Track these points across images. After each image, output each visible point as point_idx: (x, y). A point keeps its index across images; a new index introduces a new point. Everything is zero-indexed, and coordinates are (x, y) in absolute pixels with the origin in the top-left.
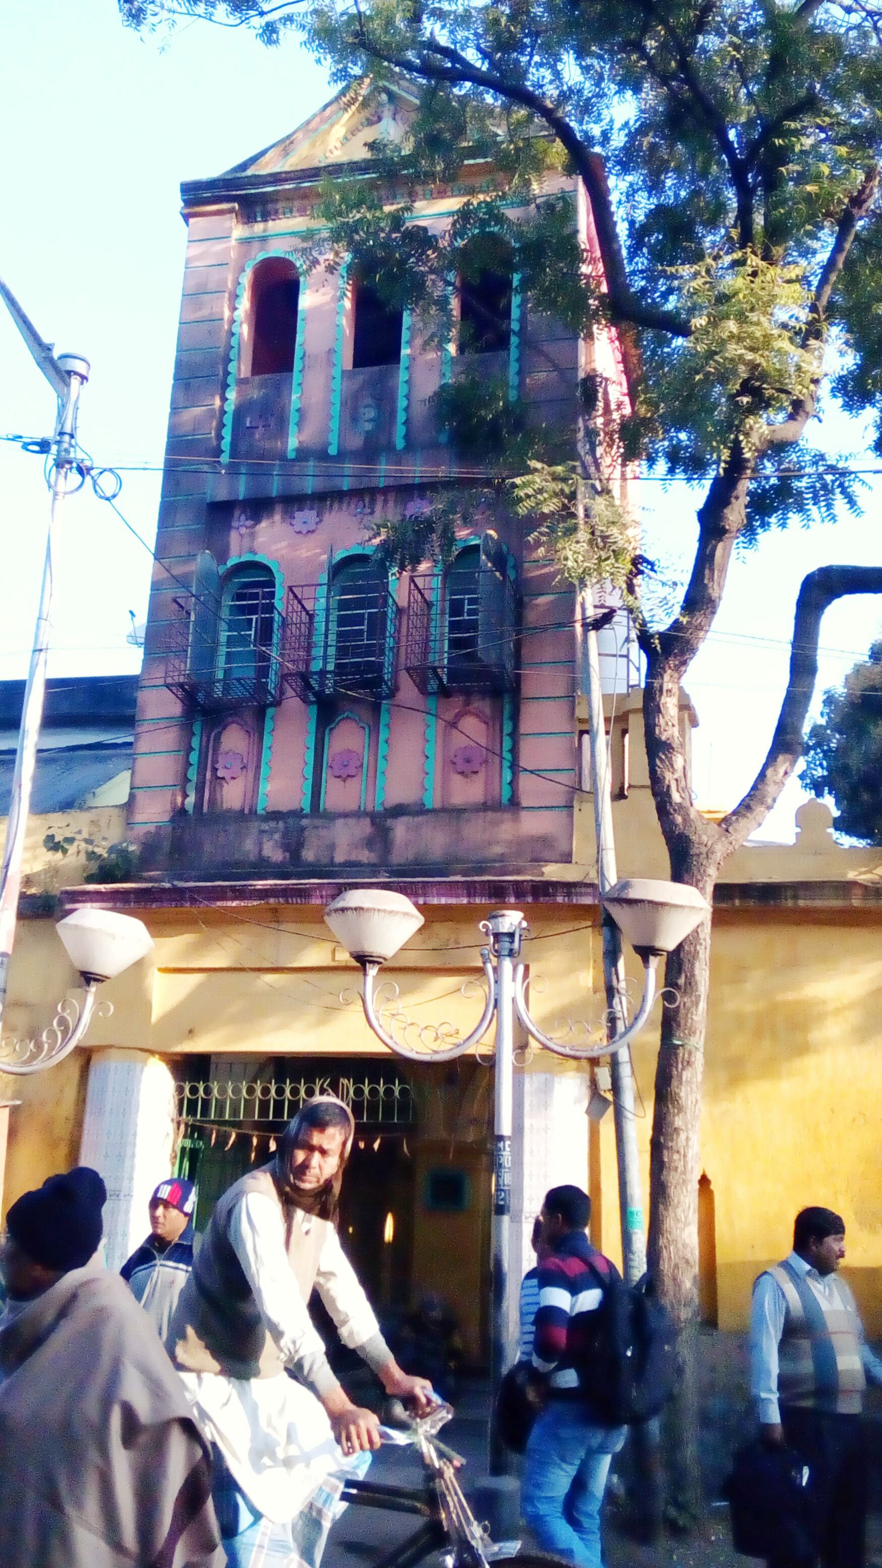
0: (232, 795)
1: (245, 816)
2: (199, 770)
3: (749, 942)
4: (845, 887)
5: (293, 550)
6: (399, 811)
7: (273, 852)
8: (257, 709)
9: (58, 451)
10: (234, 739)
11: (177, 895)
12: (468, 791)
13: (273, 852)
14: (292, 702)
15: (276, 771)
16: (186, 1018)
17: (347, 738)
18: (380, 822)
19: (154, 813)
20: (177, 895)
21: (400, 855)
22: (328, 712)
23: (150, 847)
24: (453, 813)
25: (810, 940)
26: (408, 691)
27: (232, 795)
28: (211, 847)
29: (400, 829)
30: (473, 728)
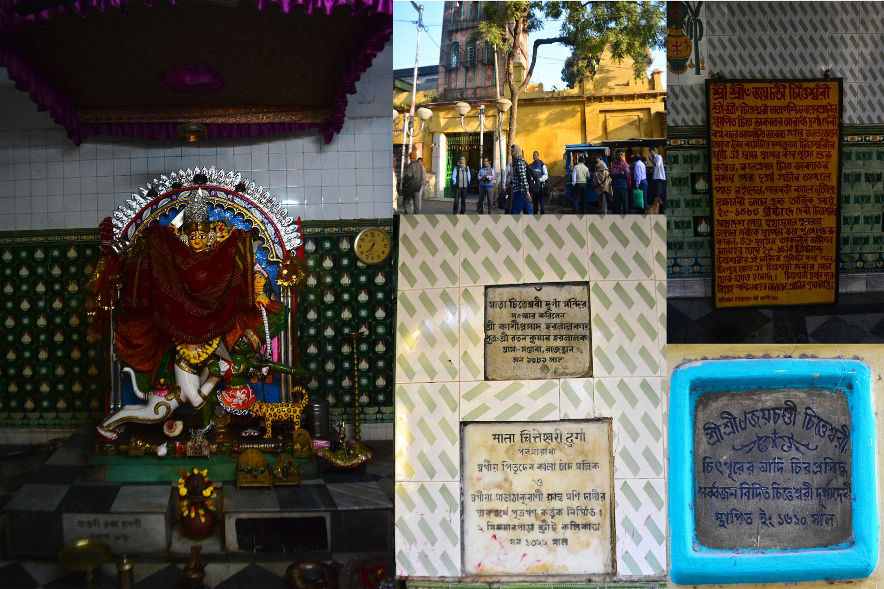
0: (453, 86)
1: (455, 89)
2: (448, 81)
3: (529, 109)
4: (543, 98)
5: (461, 38)
6: (478, 87)
7: (459, 97)
8: (457, 69)
9: (420, 24)
10: (453, 75)
11: (443, 105)
12: (489, 83)
13: (459, 97)
14: (462, 68)
15: (459, 81)
16: (447, 126)
17: (470, 74)
18: (475, 89)
19: (441, 89)
20: (443, 105)
21: (478, 96)
22: (467, 69)
23: (441, 96)
24: (486, 87)
25: (539, 108)
26: (479, 65)
27: (453, 86)
28: (449, 95)
29: (478, 91)
30: (489, 72)
